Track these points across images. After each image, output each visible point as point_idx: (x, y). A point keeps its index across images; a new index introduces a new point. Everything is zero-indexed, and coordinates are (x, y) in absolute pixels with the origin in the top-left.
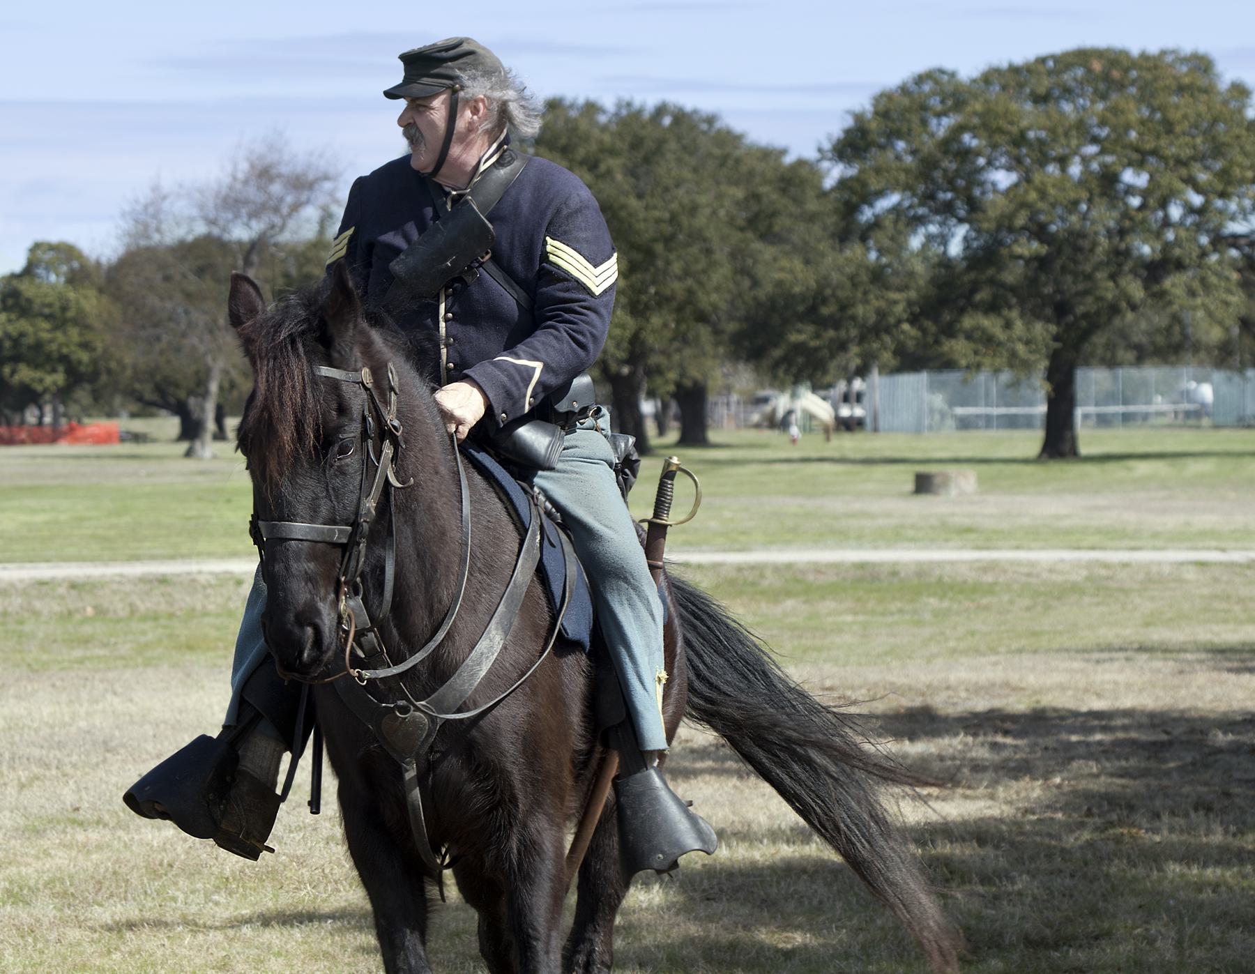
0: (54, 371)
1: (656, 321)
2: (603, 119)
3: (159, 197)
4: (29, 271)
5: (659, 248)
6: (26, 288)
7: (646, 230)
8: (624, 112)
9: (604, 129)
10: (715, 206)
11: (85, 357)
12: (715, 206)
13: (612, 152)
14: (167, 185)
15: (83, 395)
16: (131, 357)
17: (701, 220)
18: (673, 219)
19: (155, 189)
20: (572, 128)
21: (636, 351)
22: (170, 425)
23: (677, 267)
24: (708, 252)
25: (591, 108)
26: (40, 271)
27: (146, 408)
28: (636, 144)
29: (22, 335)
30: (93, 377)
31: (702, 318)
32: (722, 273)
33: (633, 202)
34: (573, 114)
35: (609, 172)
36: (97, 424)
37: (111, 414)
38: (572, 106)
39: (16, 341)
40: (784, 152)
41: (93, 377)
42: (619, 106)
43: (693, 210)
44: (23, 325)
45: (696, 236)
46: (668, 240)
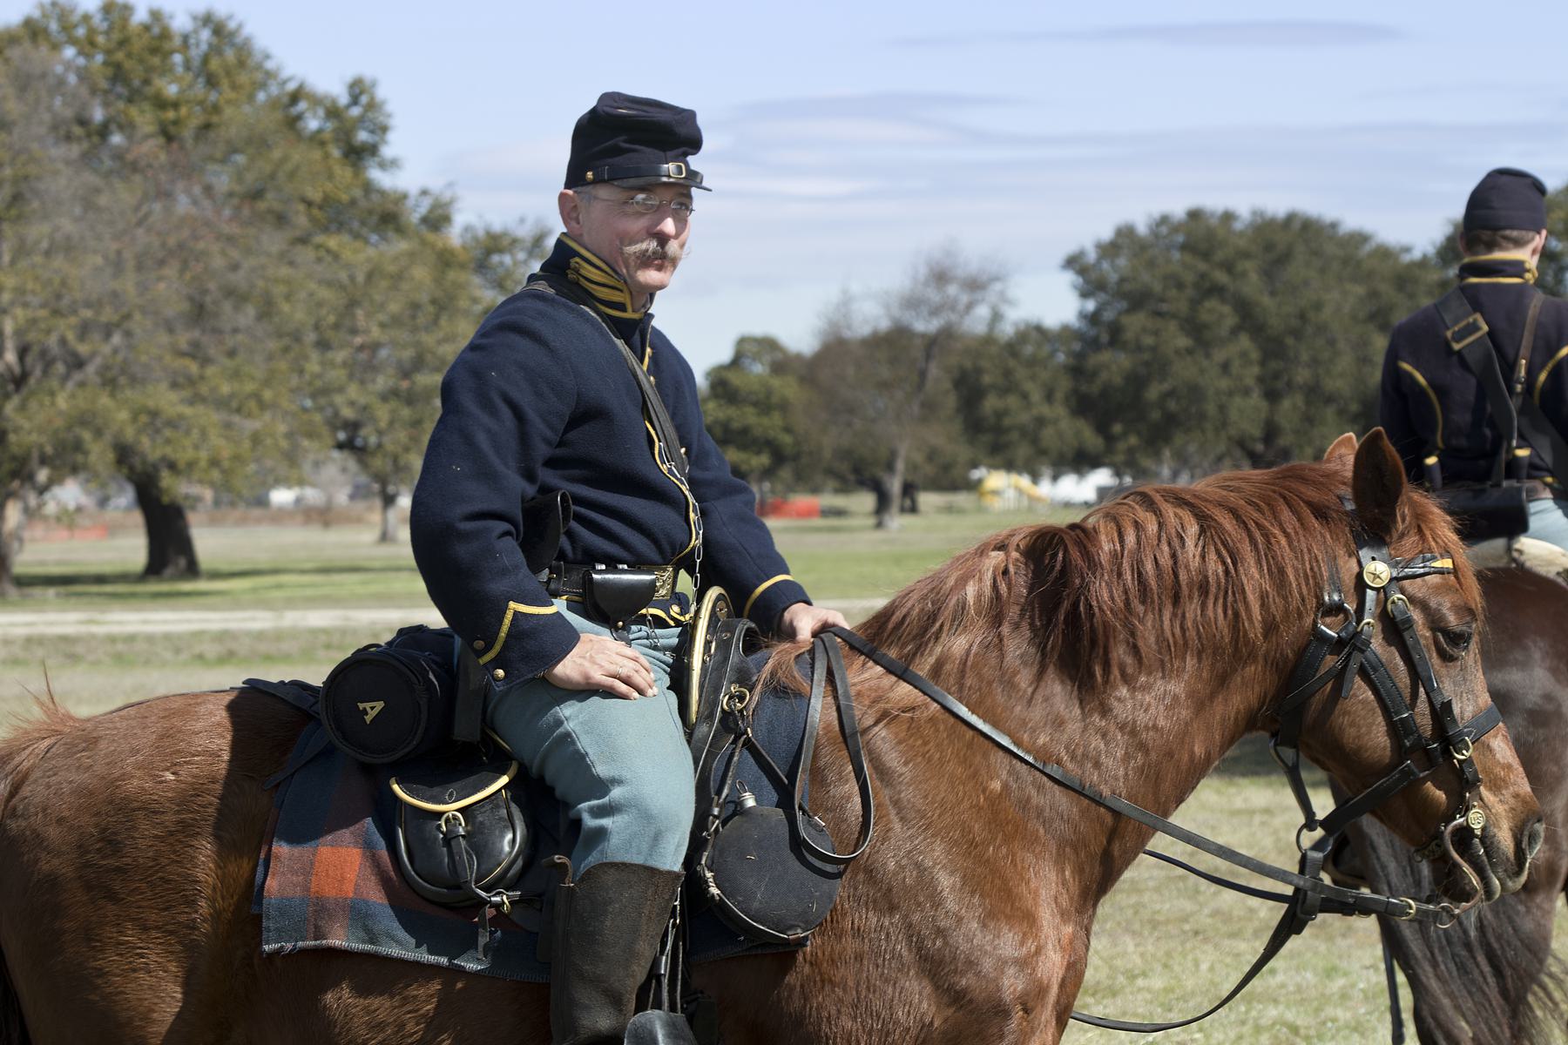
0: (759, 453)
1: (1286, 404)
2: (1238, 226)
3: (846, 301)
4: (736, 362)
5: (1290, 341)
6: (735, 379)
7: (1275, 324)
8: (1259, 220)
9: (1241, 234)
10: (1340, 302)
11: (787, 439)
12: (1340, 302)
13: (1246, 255)
14: (855, 288)
15: (786, 473)
16: (829, 441)
17: (1327, 313)
18: (1302, 316)
19: (845, 292)
20: (1211, 235)
21: (1271, 432)
22: (867, 501)
23: (1305, 357)
24: (1332, 343)
25: (1228, 217)
26: (746, 362)
27: (844, 488)
28: (1269, 247)
29: (729, 420)
30: (796, 457)
31: (1329, 399)
32: (1345, 362)
33: (1266, 300)
34: (1214, 222)
35: (1244, 274)
36: (802, 500)
37: (815, 490)
38: (1212, 214)
39: (725, 426)
40: (1407, 250)
41: (796, 457)
42: (1254, 213)
43: (1318, 306)
44: (732, 412)
45: (1321, 329)
46: (1297, 334)
